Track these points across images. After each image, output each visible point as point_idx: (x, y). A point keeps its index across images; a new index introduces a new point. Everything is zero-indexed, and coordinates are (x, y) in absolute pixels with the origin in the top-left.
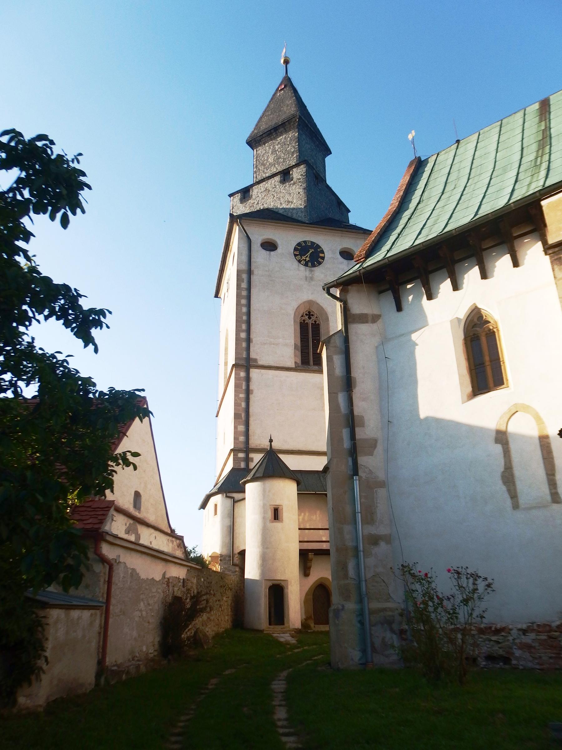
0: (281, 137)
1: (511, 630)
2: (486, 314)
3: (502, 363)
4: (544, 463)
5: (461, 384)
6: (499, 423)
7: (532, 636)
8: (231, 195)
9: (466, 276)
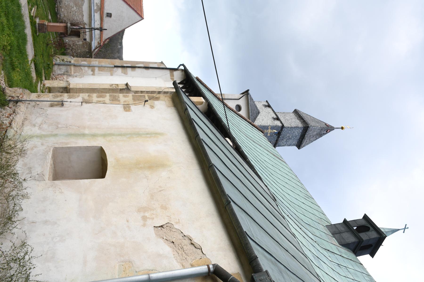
0: (299, 121)
8: (267, 101)
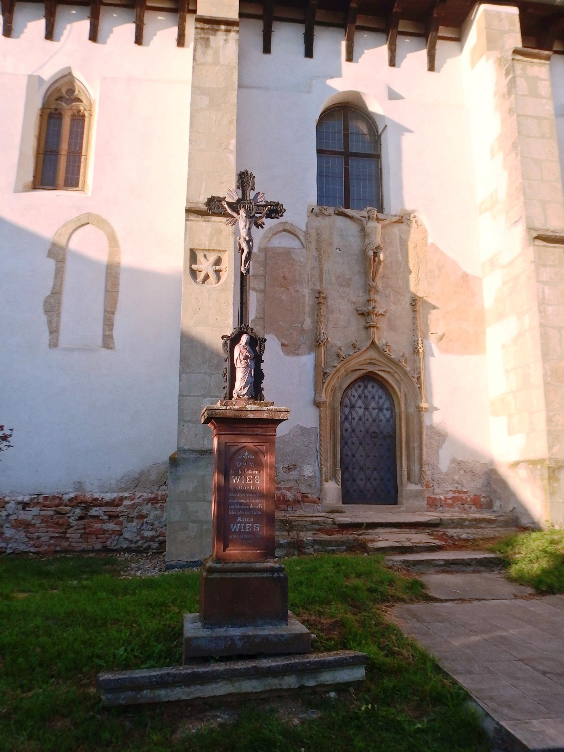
1: (7, 503)
2: (80, 87)
3: (83, 158)
4: (106, 297)
5: (20, 165)
6: (59, 232)
7: (35, 510)
9: (68, 26)
